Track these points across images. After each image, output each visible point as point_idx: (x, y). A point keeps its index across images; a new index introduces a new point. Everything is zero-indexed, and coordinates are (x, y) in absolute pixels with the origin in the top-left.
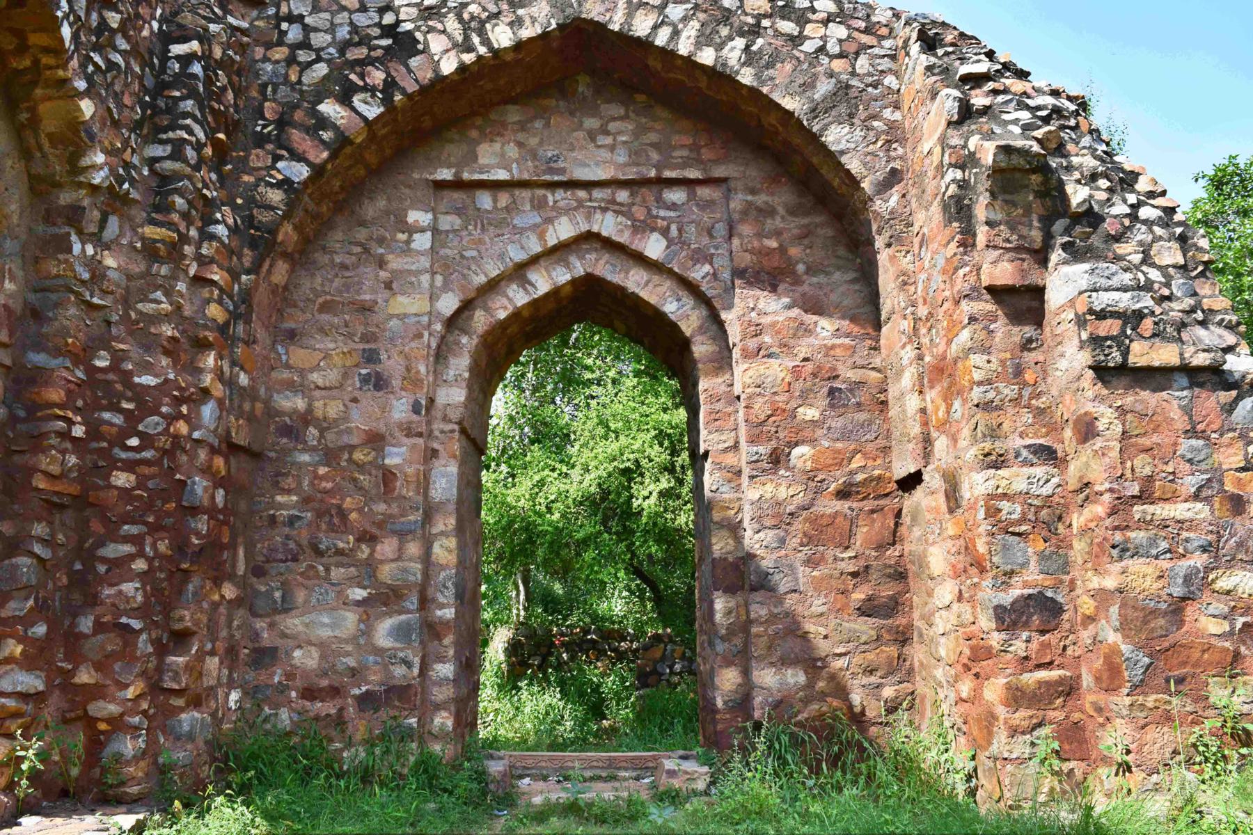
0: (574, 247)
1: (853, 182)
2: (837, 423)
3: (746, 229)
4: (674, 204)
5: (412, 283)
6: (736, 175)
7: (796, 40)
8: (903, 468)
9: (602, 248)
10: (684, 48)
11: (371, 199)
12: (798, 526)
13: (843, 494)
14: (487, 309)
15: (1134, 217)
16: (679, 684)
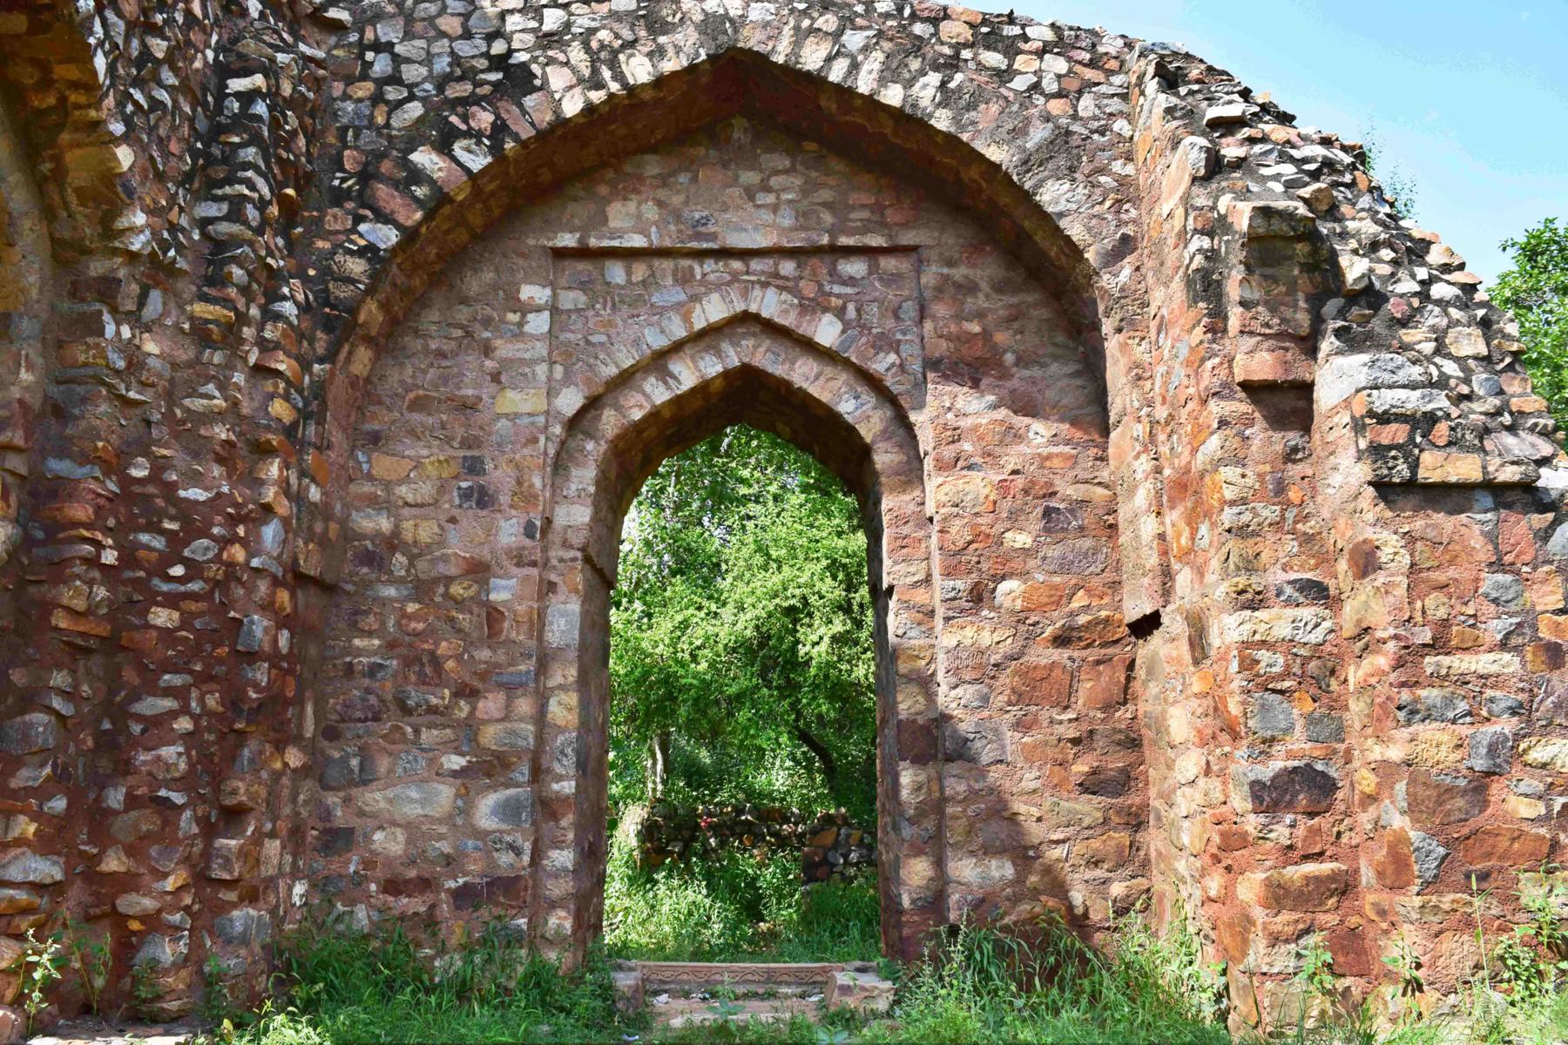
0: (726, 331)
1: (1074, 251)
2: (1054, 552)
3: (941, 310)
4: (851, 278)
5: (525, 375)
6: (929, 242)
7: (1003, 76)
8: (1136, 607)
9: (762, 332)
10: (864, 84)
11: (476, 271)
12: (1005, 679)
13: (1061, 640)
14: (618, 408)
15: (1424, 296)
16: (856, 877)
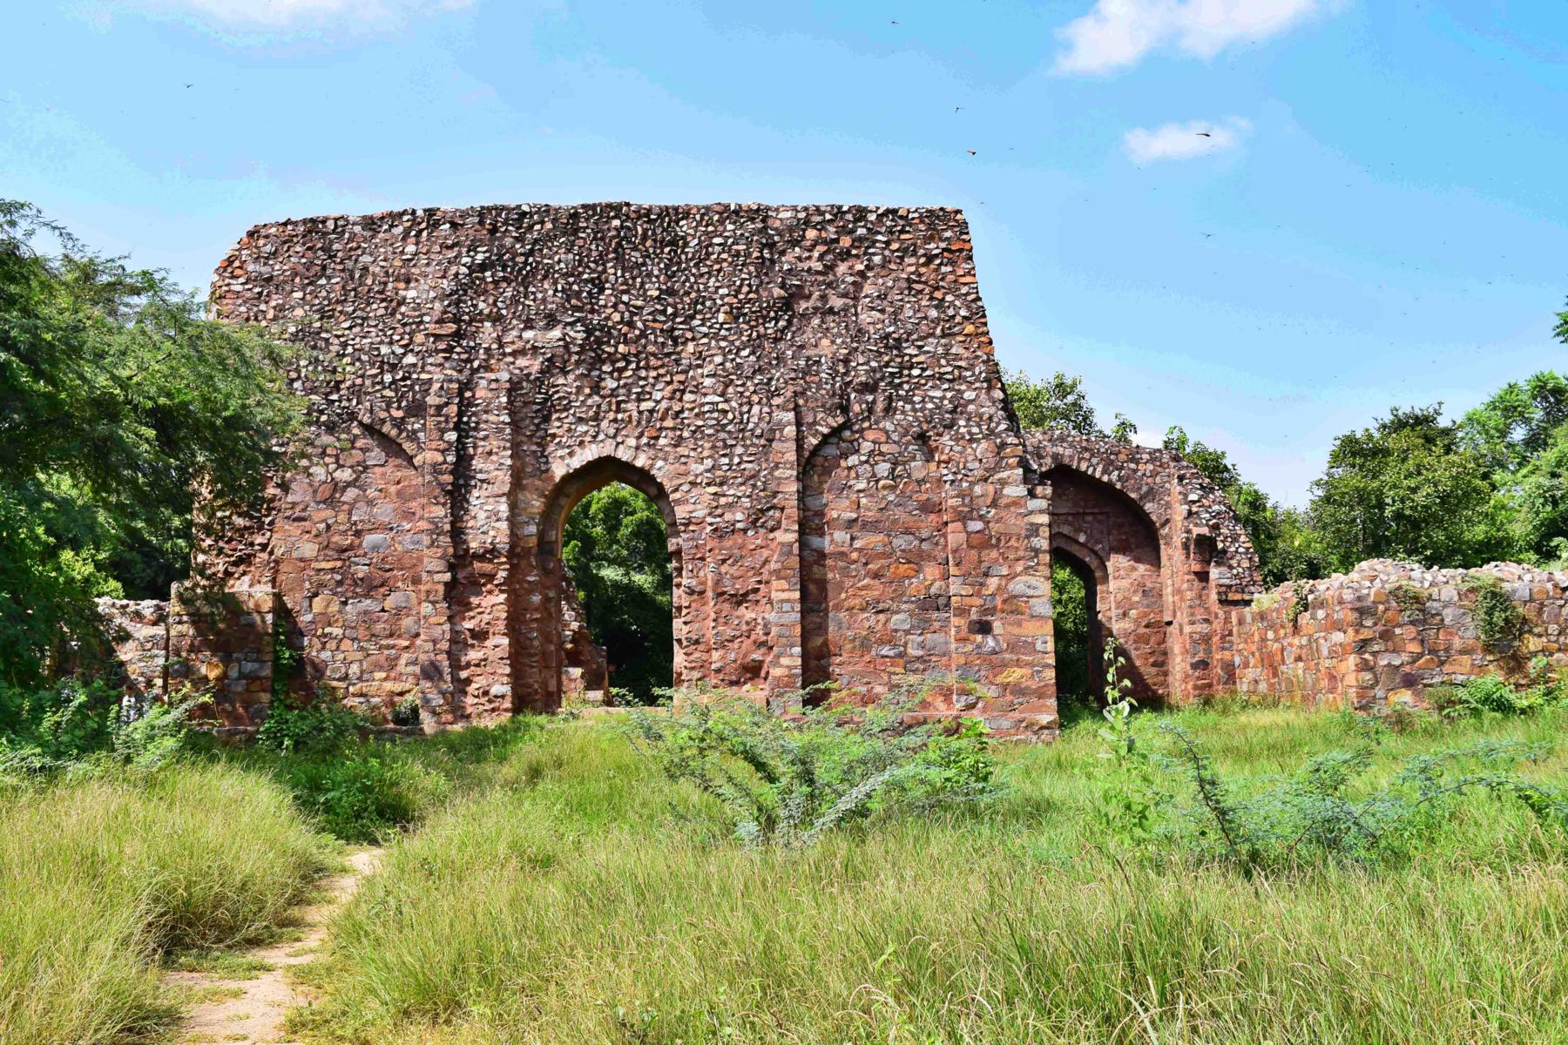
1: (1154, 523)
7: (1135, 471)
12: (1132, 637)
13: (1147, 626)
15: (1237, 552)
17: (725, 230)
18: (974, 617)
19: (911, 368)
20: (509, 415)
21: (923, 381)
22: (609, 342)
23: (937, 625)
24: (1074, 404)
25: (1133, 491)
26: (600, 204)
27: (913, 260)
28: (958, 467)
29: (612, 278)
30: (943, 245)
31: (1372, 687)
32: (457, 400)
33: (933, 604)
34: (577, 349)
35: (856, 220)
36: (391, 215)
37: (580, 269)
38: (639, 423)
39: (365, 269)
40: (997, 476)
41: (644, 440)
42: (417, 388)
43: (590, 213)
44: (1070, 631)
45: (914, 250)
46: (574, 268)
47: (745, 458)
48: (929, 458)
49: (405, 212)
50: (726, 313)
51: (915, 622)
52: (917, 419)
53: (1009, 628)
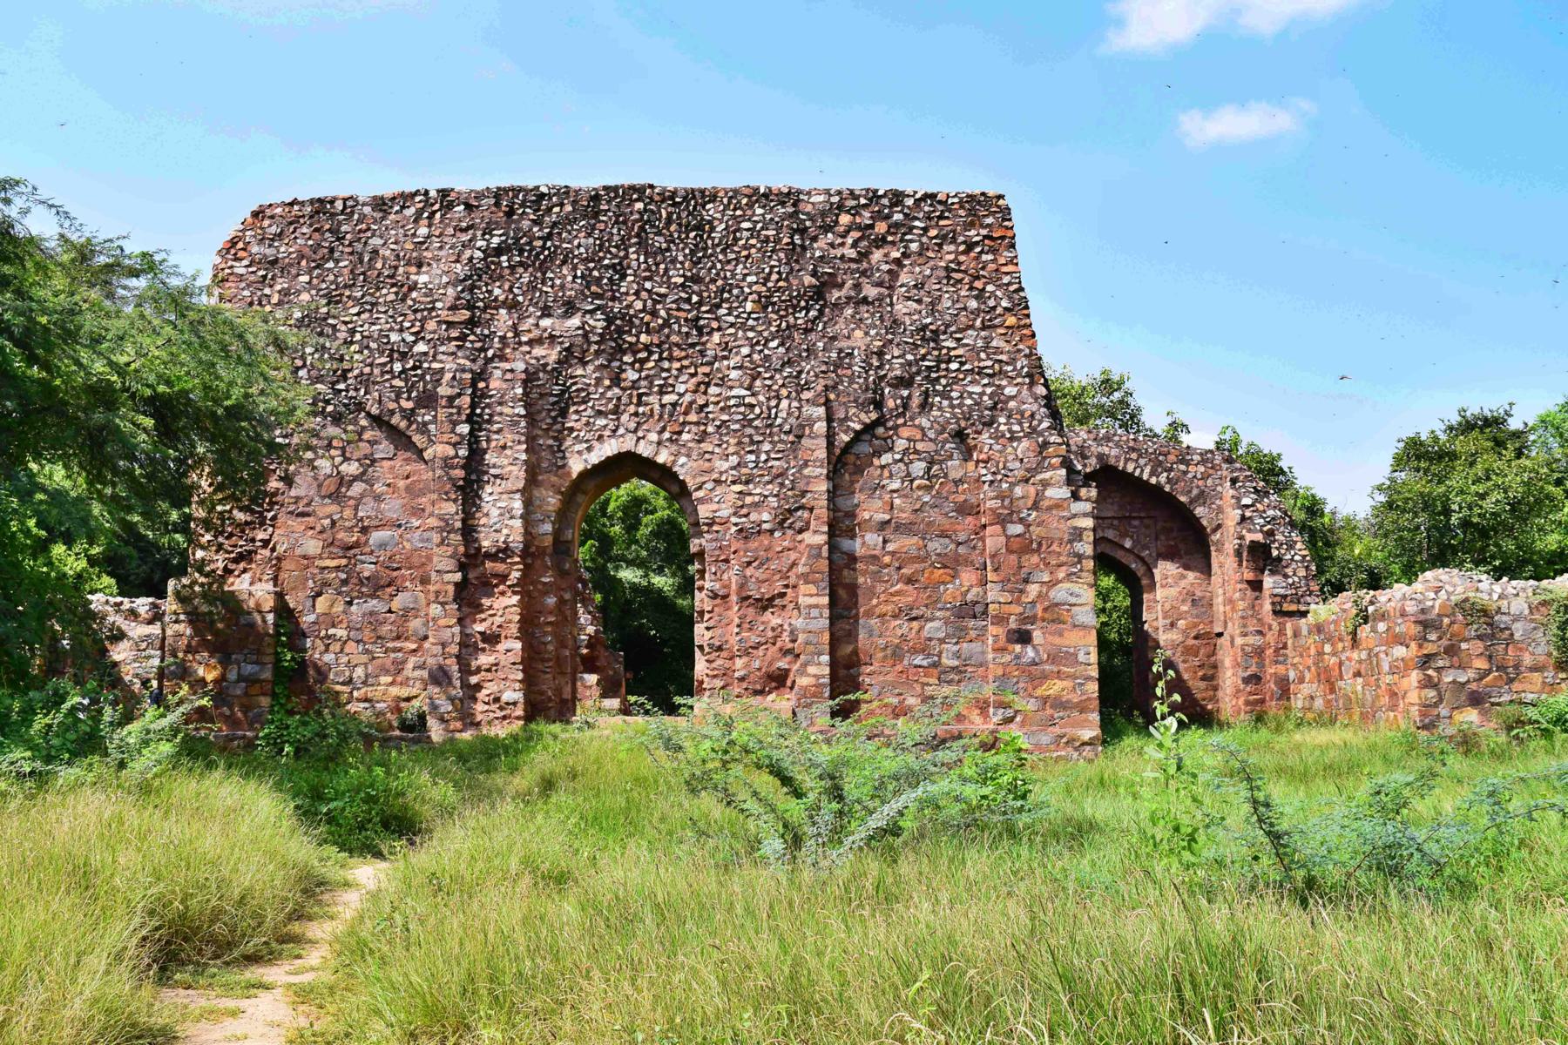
1: (1205, 528)
2: (1195, 612)
7: (1185, 473)
8: (1218, 629)
10: (1145, 477)
12: (1180, 649)
13: (1196, 638)
15: (1292, 560)
17: (754, 214)
18: (1013, 625)
19: (949, 361)
20: (525, 407)
21: (961, 376)
22: (630, 331)
23: (973, 634)
24: (1121, 402)
25: (1182, 493)
26: (623, 186)
27: (952, 248)
28: (997, 467)
29: (634, 264)
30: (984, 232)
31: (1436, 705)
32: (469, 391)
33: (970, 611)
34: (596, 338)
35: (892, 205)
36: (402, 195)
37: (601, 254)
38: (661, 416)
39: (375, 252)
40: (1039, 477)
41: (667, 435)
42: (428, 378)
43: (612, 195)
44: (1114, 642)
45: (953, 237)
46: (595, 253)
47: (773, 456)
48: (967, 456)
49: (417, 193)
50: (753, 301)
51: (950, 631)
52: (954, 415)
53: (1050, 638)
